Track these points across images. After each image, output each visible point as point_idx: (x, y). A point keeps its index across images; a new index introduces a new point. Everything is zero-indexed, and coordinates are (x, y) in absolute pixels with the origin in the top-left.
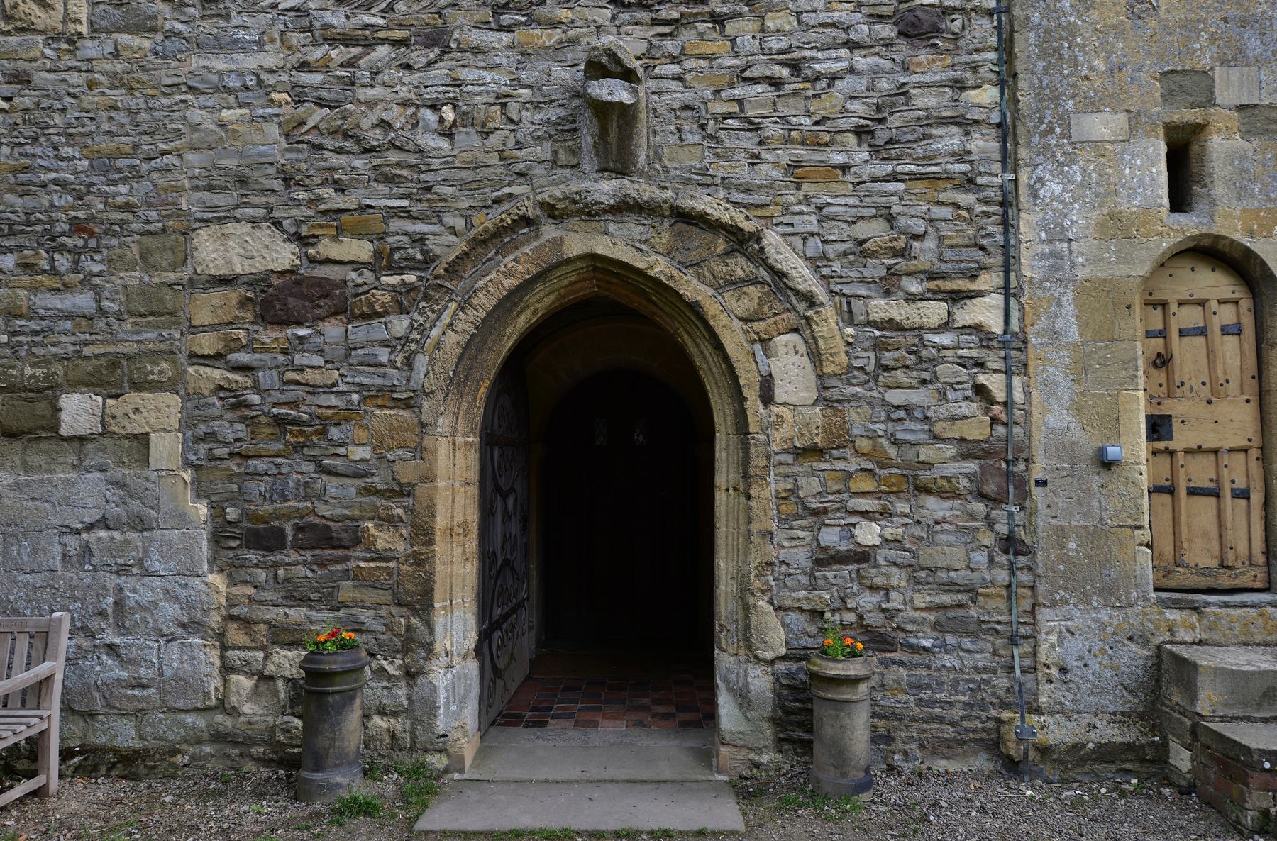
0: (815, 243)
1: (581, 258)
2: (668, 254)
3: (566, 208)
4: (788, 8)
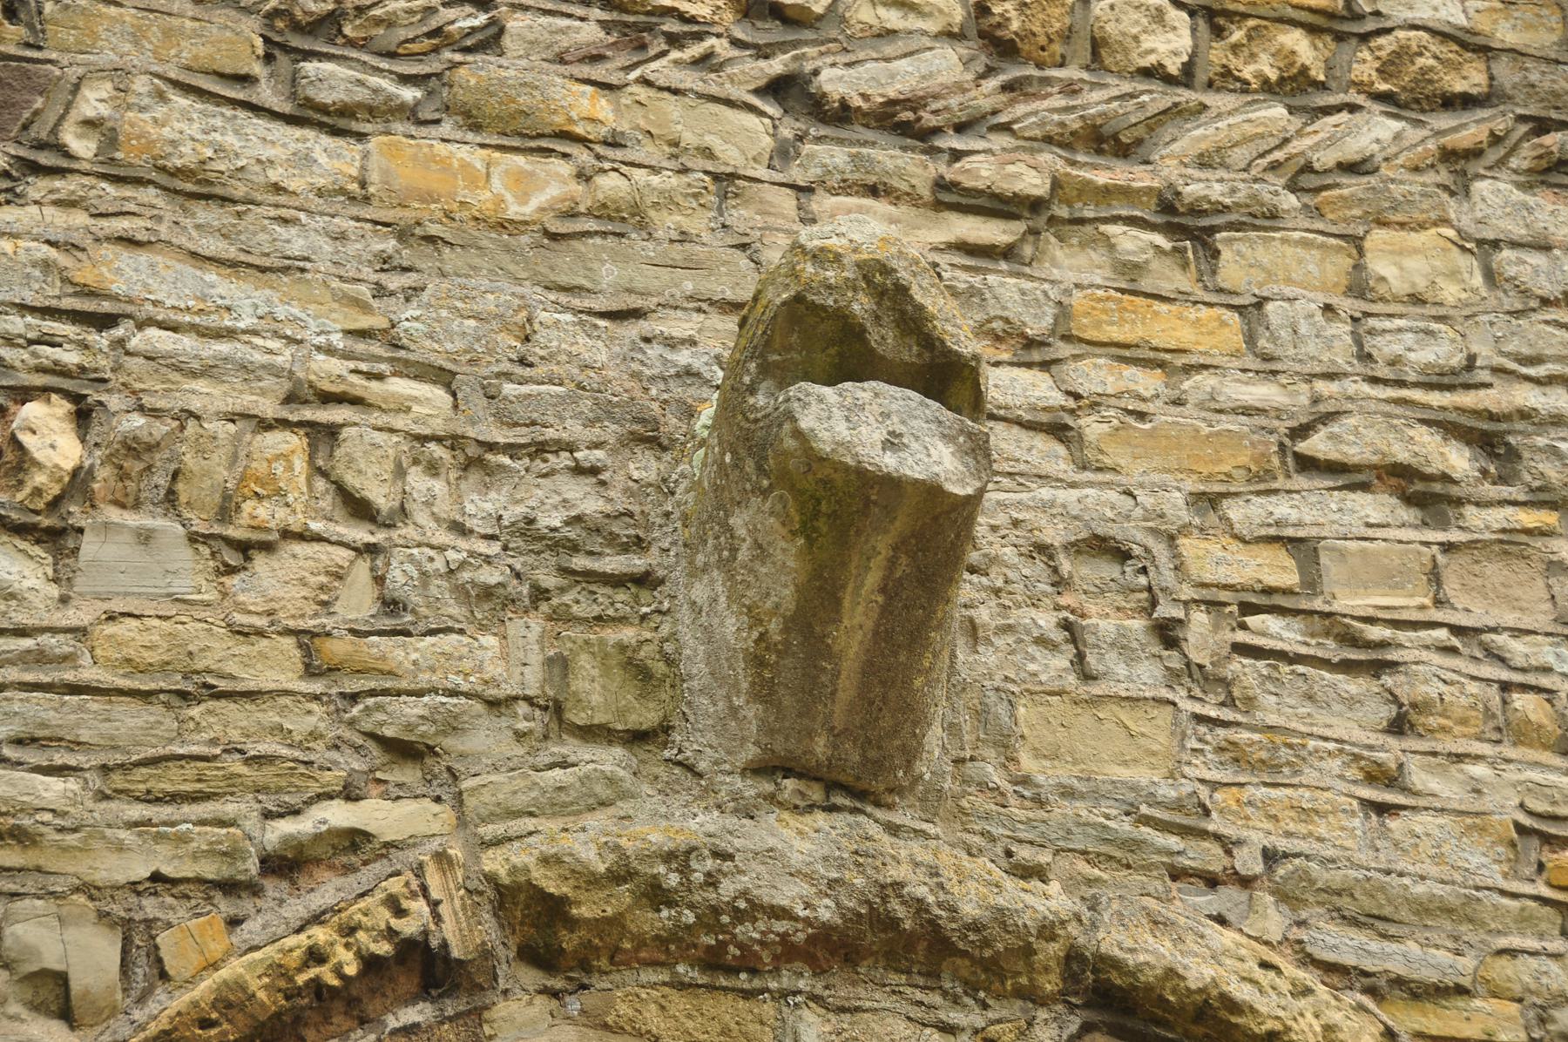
3: (616, 921)
4: (1445, 221)
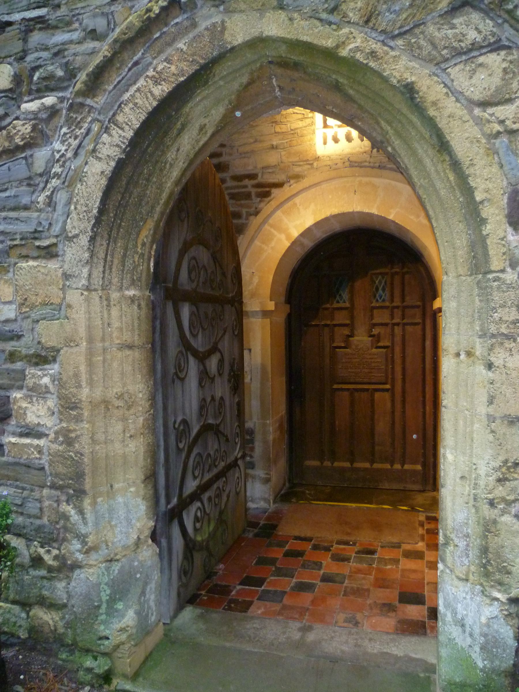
2: (367, 22)
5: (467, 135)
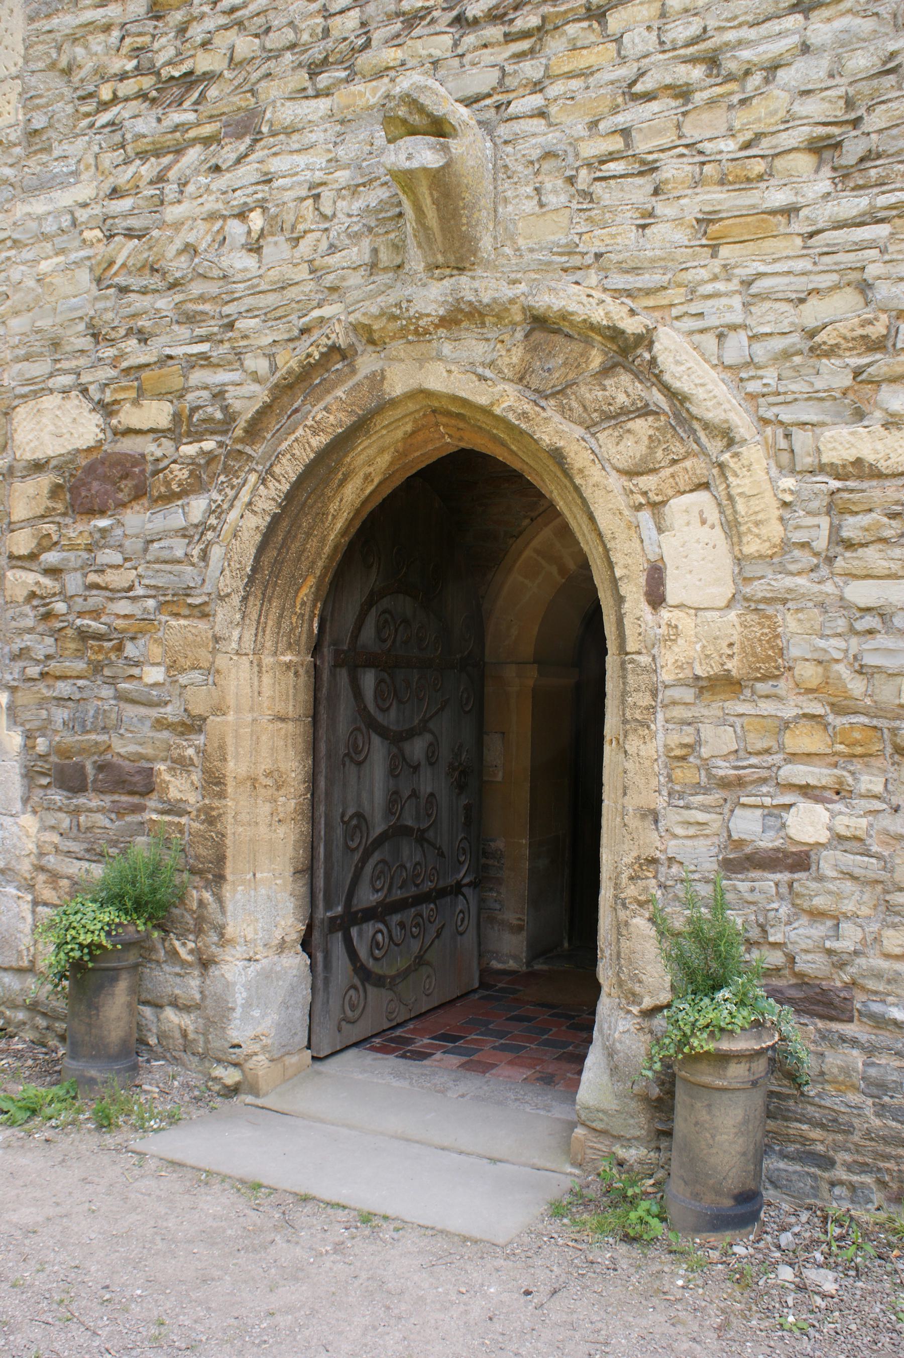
0: (737, 344)
1: (412, 395)
2: (521, 379)
5: (610, 506)
